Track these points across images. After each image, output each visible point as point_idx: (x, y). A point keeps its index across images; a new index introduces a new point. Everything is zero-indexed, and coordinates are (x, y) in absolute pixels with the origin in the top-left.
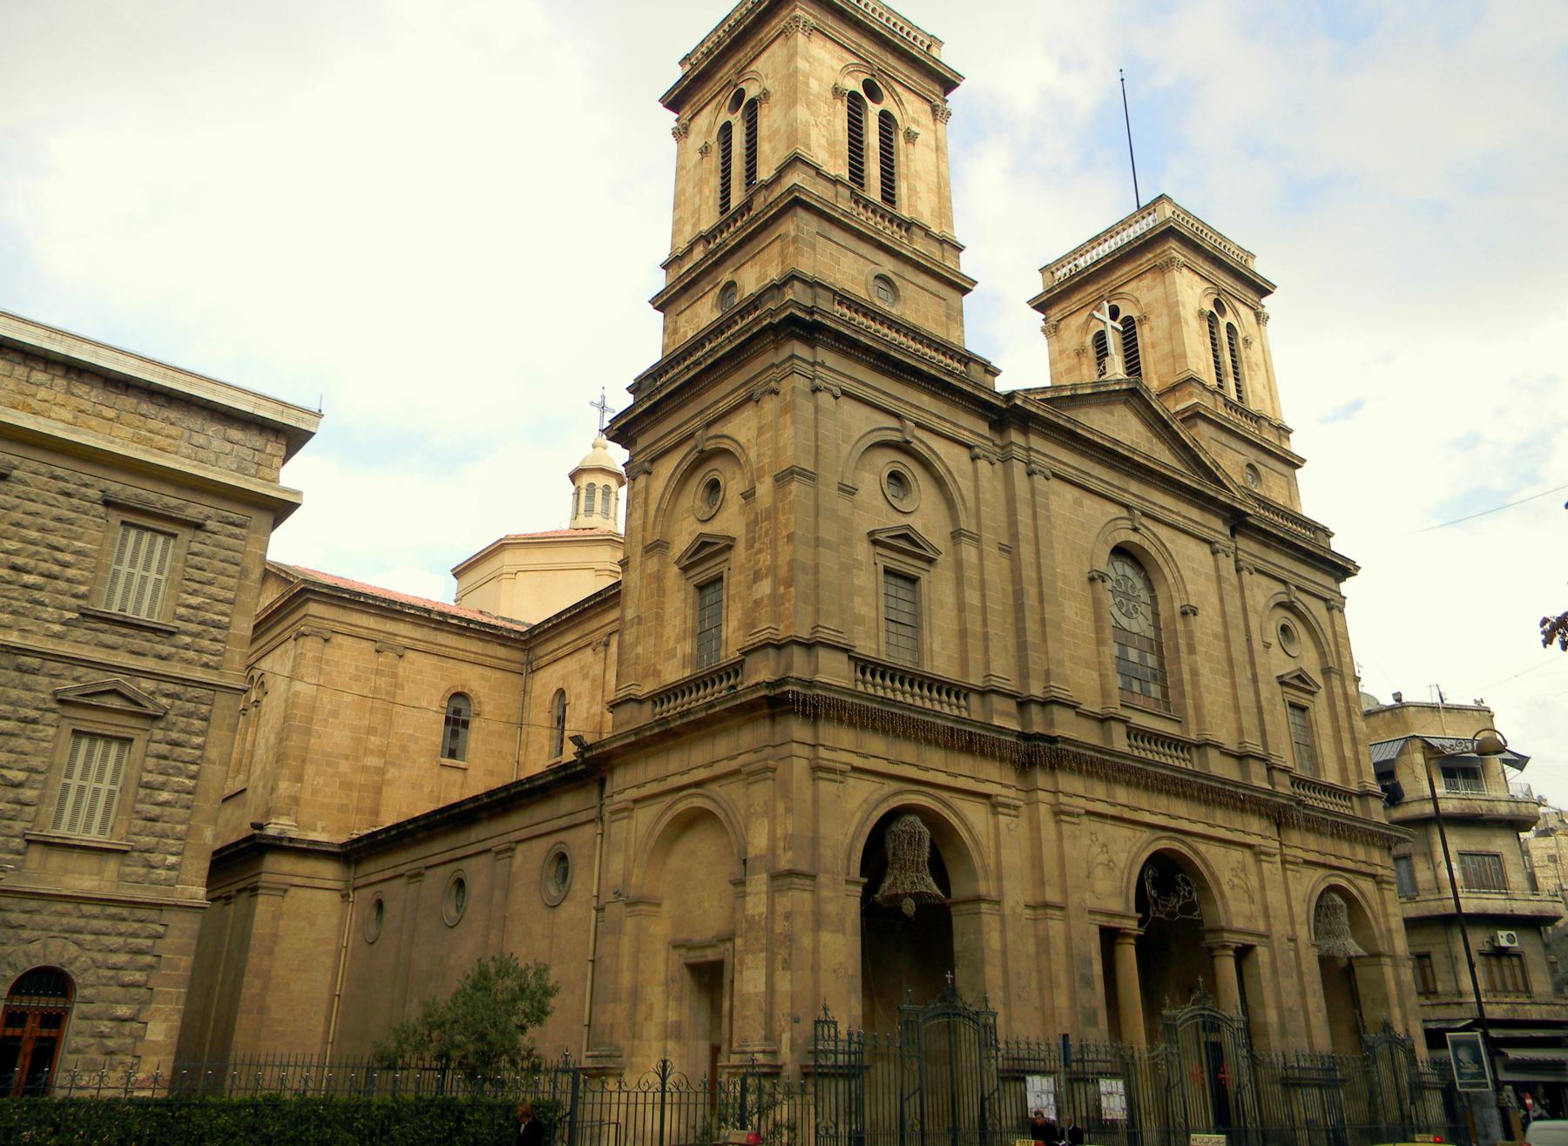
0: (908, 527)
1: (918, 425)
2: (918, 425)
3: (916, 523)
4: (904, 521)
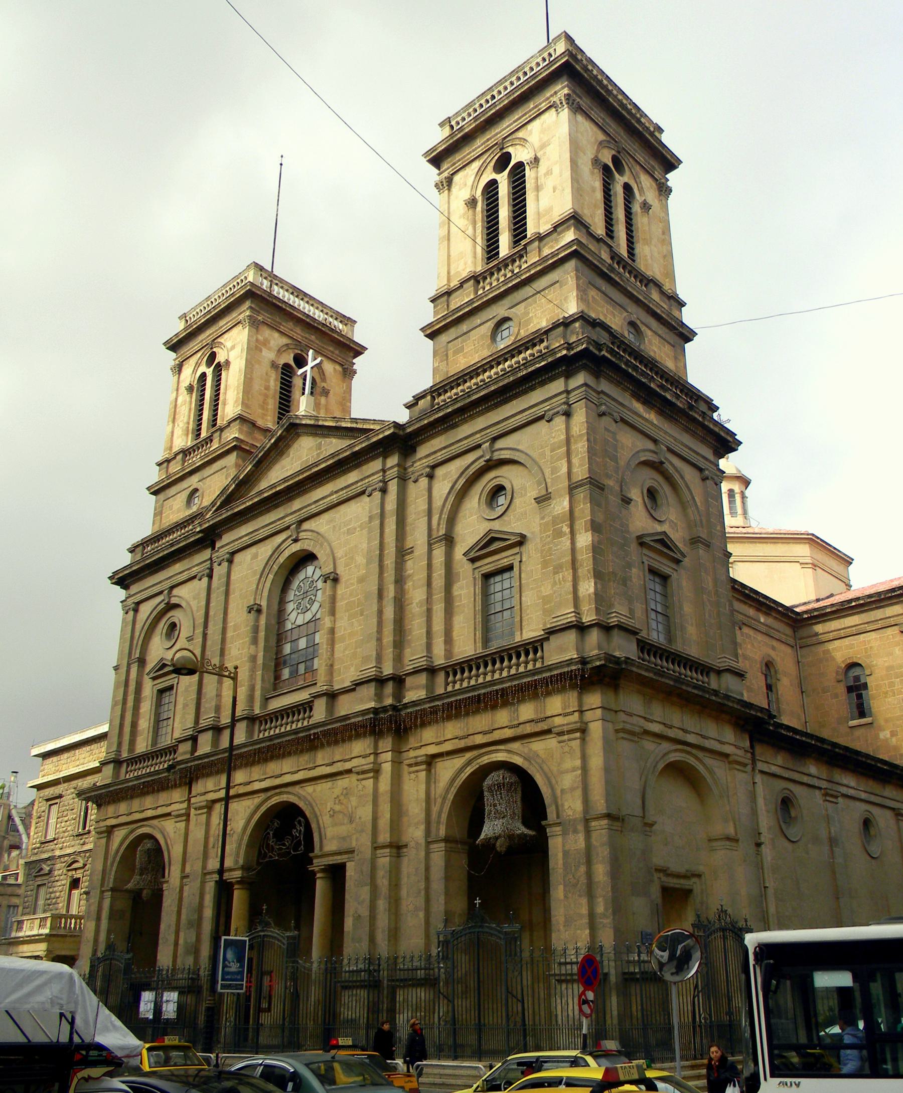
1: (670, 450)
2: (670, 450)
3: (665, 528)
4: (659, 528)
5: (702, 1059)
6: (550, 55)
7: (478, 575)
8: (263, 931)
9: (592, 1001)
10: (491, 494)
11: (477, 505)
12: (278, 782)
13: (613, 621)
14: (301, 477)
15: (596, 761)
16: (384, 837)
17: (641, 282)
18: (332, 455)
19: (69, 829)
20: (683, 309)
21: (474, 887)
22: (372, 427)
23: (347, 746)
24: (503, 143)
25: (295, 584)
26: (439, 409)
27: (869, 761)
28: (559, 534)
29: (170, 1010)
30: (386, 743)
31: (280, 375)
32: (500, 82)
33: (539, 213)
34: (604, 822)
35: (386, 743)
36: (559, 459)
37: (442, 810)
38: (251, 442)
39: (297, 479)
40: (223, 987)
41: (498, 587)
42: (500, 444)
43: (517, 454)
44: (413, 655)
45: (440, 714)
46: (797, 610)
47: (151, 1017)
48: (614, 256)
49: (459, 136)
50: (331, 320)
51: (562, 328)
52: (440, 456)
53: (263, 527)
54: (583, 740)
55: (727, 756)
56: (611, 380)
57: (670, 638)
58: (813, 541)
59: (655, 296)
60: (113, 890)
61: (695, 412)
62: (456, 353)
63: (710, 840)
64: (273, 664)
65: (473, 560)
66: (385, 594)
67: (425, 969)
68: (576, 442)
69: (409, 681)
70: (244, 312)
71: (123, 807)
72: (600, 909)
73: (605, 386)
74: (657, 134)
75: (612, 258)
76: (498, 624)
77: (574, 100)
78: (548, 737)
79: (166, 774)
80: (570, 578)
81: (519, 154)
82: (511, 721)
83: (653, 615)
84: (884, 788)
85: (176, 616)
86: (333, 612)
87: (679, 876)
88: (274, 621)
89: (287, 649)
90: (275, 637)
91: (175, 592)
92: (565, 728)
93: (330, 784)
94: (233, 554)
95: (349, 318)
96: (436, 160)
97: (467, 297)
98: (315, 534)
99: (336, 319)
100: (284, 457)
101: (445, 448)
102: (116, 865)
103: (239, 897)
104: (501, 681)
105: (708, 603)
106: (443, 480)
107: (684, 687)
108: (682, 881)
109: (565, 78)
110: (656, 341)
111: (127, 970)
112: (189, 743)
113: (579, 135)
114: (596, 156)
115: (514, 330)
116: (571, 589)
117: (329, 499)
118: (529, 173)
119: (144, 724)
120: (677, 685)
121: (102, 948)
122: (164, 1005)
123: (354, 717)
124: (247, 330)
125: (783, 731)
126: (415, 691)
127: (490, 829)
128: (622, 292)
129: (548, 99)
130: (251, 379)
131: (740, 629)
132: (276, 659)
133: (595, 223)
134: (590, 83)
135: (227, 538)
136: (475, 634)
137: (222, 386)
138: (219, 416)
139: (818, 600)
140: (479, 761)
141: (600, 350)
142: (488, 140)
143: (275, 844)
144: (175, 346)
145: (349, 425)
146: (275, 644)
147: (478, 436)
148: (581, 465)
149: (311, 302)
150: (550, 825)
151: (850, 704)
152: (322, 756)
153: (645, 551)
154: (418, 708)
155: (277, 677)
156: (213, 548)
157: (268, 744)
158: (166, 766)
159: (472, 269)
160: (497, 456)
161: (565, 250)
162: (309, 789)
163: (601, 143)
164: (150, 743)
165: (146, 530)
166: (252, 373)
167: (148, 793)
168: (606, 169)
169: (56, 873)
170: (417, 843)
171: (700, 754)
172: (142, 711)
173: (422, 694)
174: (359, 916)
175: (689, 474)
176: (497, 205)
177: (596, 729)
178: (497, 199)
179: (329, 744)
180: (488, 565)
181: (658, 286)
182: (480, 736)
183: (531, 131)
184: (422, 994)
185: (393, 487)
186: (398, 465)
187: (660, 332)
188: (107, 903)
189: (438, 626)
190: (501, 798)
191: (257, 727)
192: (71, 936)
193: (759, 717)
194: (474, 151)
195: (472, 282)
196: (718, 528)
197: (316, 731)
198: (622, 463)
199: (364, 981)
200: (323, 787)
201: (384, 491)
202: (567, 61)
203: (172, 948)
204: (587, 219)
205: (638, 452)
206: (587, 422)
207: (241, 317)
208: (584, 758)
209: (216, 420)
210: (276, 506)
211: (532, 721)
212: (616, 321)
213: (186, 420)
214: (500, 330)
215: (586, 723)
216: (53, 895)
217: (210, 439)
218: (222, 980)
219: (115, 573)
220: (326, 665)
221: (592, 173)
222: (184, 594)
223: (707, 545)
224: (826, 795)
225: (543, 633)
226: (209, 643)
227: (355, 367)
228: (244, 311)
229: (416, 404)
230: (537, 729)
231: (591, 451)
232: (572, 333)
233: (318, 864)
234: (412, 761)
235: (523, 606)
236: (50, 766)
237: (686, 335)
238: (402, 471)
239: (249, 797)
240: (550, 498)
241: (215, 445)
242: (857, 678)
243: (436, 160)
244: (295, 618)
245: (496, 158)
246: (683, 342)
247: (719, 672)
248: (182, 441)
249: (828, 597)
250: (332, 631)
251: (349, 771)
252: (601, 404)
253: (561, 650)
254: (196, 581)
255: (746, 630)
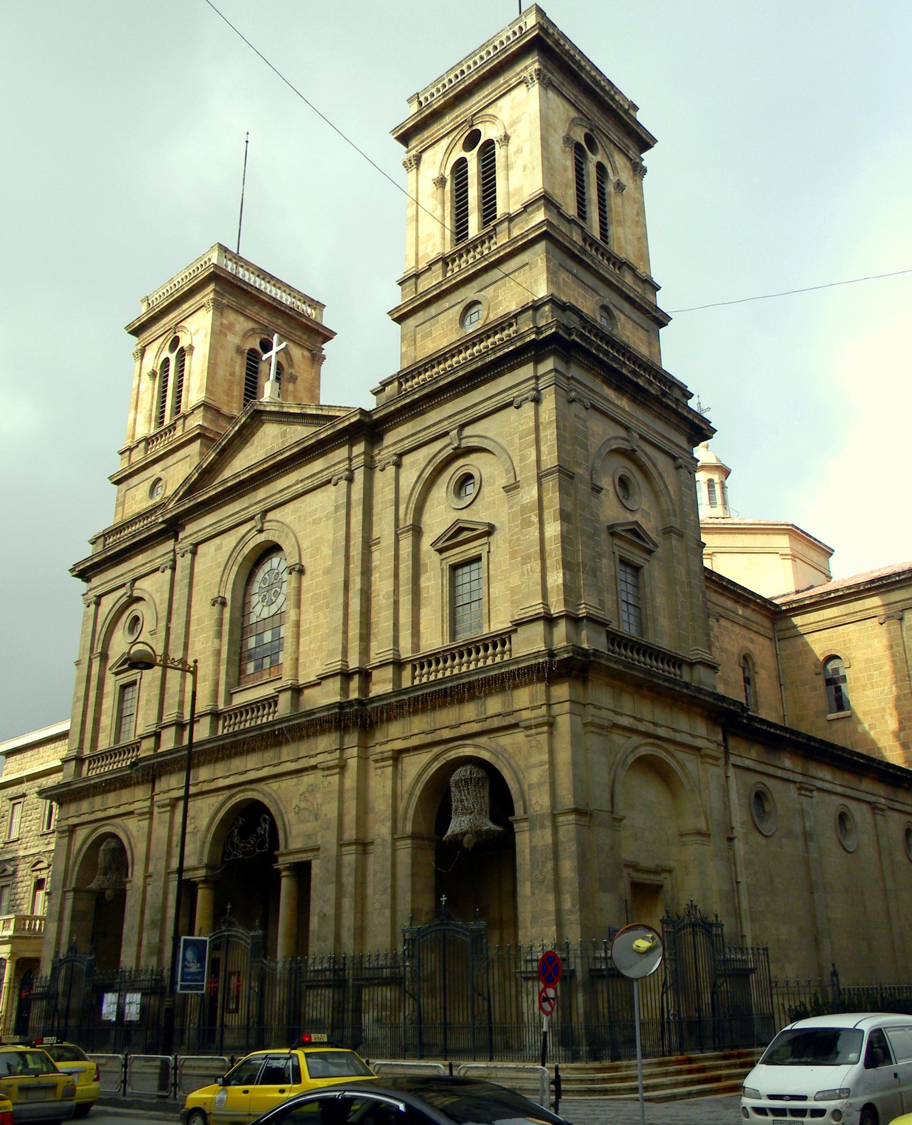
0: (636, 523)
1: (642, 437)
2: (642, 437)
3: (637, 517)
4: (631, 518)
5: (670, 1056)
6: (521, 28)
7: (446, 567)
8: (228, 931)
9: (552, 998)
10: (459, 483)
11: (445, 494)
12: (242, 778)
13: (582, 612)
14: (265, 466)
15: (564, 756)
16: (350, 834)
17: (614, 264)
18: (297, 443)
19: (33, 828)
20: (657, 293)
21: (441, 884)
22: (337, 414)
23: (312, 741)
24: (472, 121)
25: (261, 575)
26: (407, 395)
27: (845, 755)
28: (527, 523)
29: (133, 1012)
30: (352, 739)
31: (246, 361)
32: (469, 57)
33: (508, 193)
34: (572, 817)
35: (352, 739)
36: (528, 446)
37: (409, 807)
38: (215, 429)
39: (261, 468)
40: (183, 988)
41: (466, 578)
42: (467, 431)
43: (486, 441)
44: (379, 648)
45: (406, 708)
46: (776, 602)
47: (114, 1019)
48: (586, 237)
49: (427, 112)
50: (299, 303)
51: (531, 312)
52: (407, 444)
53: (228, 517)
54: (551, 734)
55: (698, 749)
56: (580, 365)
57: (642, 630)
58: (793, 532)
59: (629, 279)
60: (75, 890)
61: (669, 399)
62: (424, 337)
63: (681, 835)
64: (238, 658)
65: (441, 551)
66: (351, 586)
67: (391, 968)
68: (545, 429)
69: (375, 674)
70: (208, 295)
71: (85, 806)
72: (567, 905)
73: (575, 371)
74: (631, 112)
75: (584, 240)
76: (466, 616)
77: (545, 76)
78: (515, 731)
79: (128, 772)
80: (539, 569)
81: (488, 132)
82: (478, 715)
83: (624, 606)
84: (861, 782)
85: (138, 609)
86: (298, 605)
87: (648, 872)
88: (238, 614)
89: (252, 642)
90: (240, 630)
91: (138, 584)
92: (533, 722)
93: (295, 780)
94: (196, 545)
95: (318, 302)
96: (405, 138)
97: (436, 280)
98: (280, 525)
99: (304, 303)
100: (248, 445)
101: (412, 435)
102: (78, 864)
103: (203, 896)
104: (469, 674)
105: (680, 595)
106: (411, 468)
107: (655, 680)
108: (652, 877)
109: (536, 53)
110: (629, 325)
111: (90, 973)
112: (153, 740)
113: (550, 112)
114: (568, 134)
115: (483, 314)
116: (539, 580)
117: (294, 488)
118: (499, 152)
119: (107, 720)
120: (647, 677)
121: (64, 949)
122: (127, 1007)
123: (319, 712)
124: (211, 313)
125: (756, 725)
126: (381, 685)
127: (457, 825)
128: (594, 275)
129: (518, 74)
130: (216, 364)
131: (718, 621)
132: (241, 653)
133: (566, 204)
134: (562, 58)
135: (190, 528)
136: (443, 627)
137: (186, 373)
138: (182, 404)
139: (797, 592)
140: (446, 756)
141: (570, 335)
142: (457, 117)
143: (240, 842)
144: (137, 331)
145: (314, 412)
146: (239, 638)
147: (446, 423)
148: (550, 453)
149: (278, 285)
150: (517, 821)
151: (828, 697)
152: (287, 752)
153: (617, 541)
154: (384, 702)
155: (241, 671)
156: (177, 540)
157: (233, 739)
158: (129, 763)
159: (441, 251)
160: (465, 443)
161: (534, 231)
162: (274, 785)
163: (573, 120)
164: (112, 740)
165: (109, 521)
166: (216, 358)
167: (110, 791)
168: (578, 148)
169: (20, 874)
170: (384, 840)
171: (671, 748)
172: (104, 707)
173: (388, 688)
174: (325, 915)
175: (663, 463)
176: (467, 184)
177: (564, 722)
178: (467, 178)
179: (294, 740)
180: (456, 555)
181: (633, 269)
182: (447, 730)
183: (501, 108)
184: (387, 993)
185: (359, 476)
186: (364, 453)
187: (633, 317)
188: (69, 903)
189: (405, 618)
190: (468, 793)
191: (221, 723)
192: (35, 938)
193: (731, 710)
194: (443, 128)
195: (440, 263)
196: (692, 518)
197: (280, 726)
198: (592, 451)
199: (329, 980)
200: (288, 784)
201: (350, 480)
202: (538, 34)
203: (135, 948)
204: (558, 199)
205: (609, 440)
206: (556, 408)
207: (205, 300)
208: (552, 752)
209: (180, 407)
210: (241, 496)
211: (500, 715)
212: (588, 305)
213: (148, 407)
214: (469, 314)
215: (554, 717)
216: (17, 896)
217: (173, 427)
218: (181, 981)
219: (77, 565)
220: (291, 659)
221: (564, 152)
222: (145, 586)
223: (681, 535)
224: (800, 789)
225: (510, 625)
226: (172, 637)
227: (324, 353)
228: (208, 294)
229: (383, 390)
230: (505, 724)
231: (560, 438)
232: (542, 316)
233: (283, 862)
234: (379, 757)
235: (491, 597)
236: (14, 764)
237: (661, 320)
238: (369, 459)
239: (214, 794)
240: (518, 487)
241: (179, 432)
242: (836, 670)
243: (405, 138)
244: (259, 611)
245: (466, 135)
246: (656, 327)
247: (691, 665)
248: (145, 429)
249: (808, 589)
250: (298, 624)
251: (314, 767)
252: (571, 391)
253: (529, 642)
254: (159, 573)
255: (723, 622)
